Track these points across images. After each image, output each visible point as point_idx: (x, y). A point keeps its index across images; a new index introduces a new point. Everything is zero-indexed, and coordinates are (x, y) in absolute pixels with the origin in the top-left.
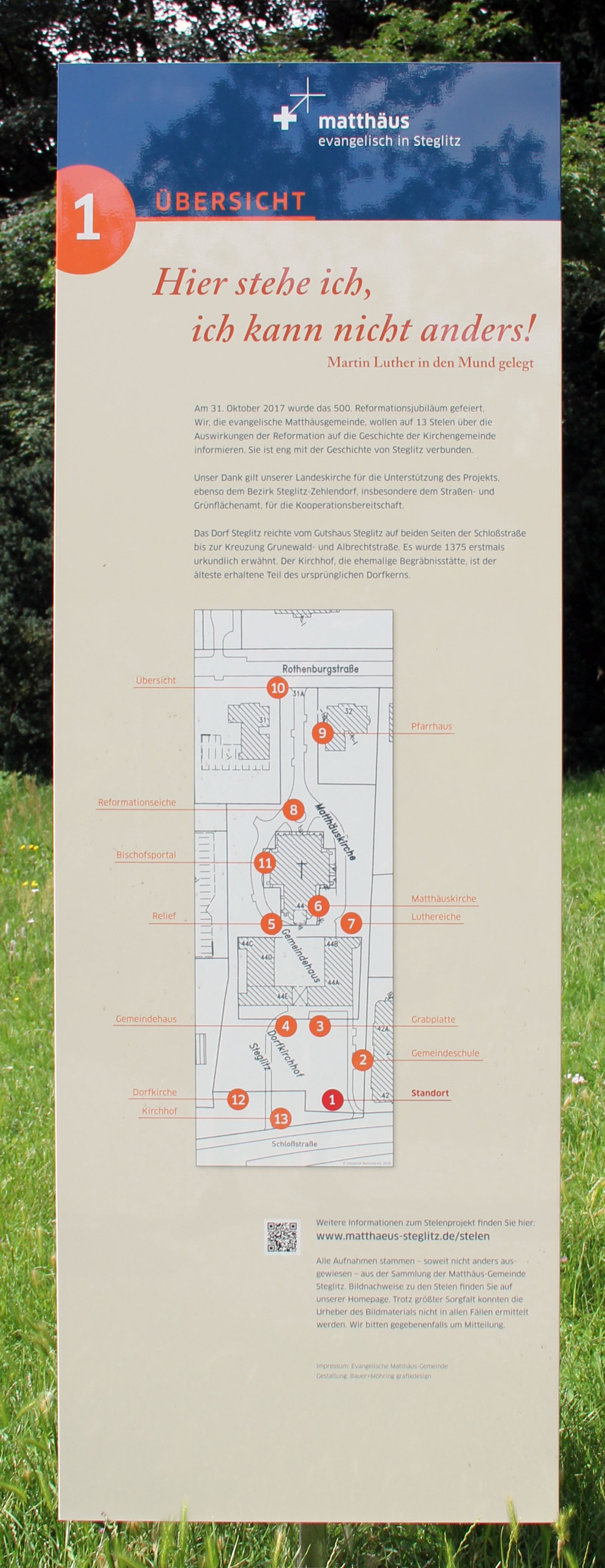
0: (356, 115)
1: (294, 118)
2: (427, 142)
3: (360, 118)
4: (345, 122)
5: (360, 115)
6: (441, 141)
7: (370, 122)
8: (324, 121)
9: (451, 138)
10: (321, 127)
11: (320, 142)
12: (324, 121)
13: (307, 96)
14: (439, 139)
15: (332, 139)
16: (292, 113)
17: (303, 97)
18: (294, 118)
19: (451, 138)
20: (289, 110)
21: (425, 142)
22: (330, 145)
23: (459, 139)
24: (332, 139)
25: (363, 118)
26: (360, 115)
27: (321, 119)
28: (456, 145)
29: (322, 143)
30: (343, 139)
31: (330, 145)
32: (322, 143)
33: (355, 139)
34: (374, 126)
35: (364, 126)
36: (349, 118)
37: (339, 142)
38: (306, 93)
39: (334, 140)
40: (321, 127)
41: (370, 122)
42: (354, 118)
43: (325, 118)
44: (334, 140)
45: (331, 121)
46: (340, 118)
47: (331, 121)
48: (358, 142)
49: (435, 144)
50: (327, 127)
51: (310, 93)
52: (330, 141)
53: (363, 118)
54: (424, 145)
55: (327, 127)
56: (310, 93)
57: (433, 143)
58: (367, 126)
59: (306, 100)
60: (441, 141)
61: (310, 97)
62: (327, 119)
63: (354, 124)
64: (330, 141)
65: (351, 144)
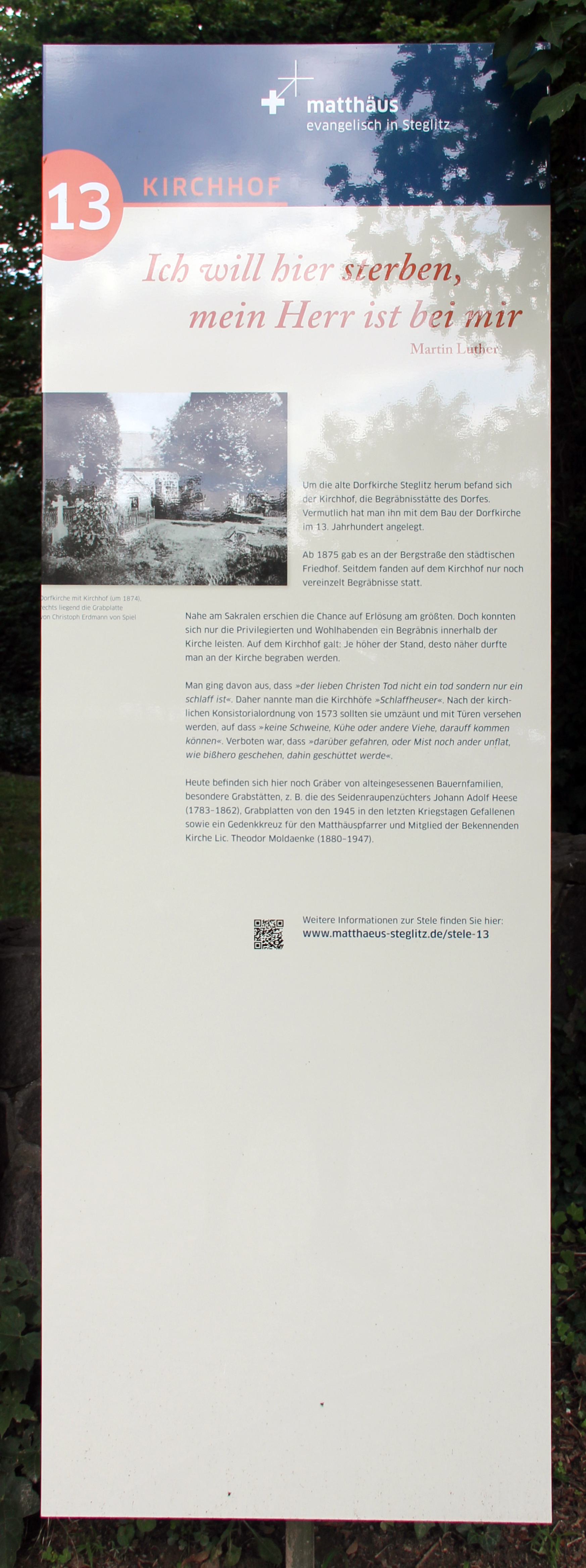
0: (344, 99)
1: (282, 102)
2: (416, 126)
3: (348, 101)
4: (333, 106)
5: (348, 99)
6: (430, 123)
7: (359, 105)
8: (312, 105)
9: (440, 122)
10: (309, 111)
11: (308, 126)
12: (312, 105)
13: (295, 79)
14: (428, 123)
15: (320, 124)
16: (280, 98)
17: (292, 80)
18: (282, 102)
19: (440, 122)
20: (277, 94)
21: (414, 127)
22: (318, 129)
23: (448, 122)
24: (320, 124)
25: (351, 102)
26: (348, 99)
27: (309, 103)
28: (445, 128)
29: (310, 128)
30: (331, 124)
31: (318, 129)
32: (310, 128)
33: (343, 123)
34: (362, 110)
35: (353, 110)
36: (338, 102)
37: (328, 126)
38: (294, 77)
39: (322, 125)
40: (309, 111)
41: (359, 105)
42: (343, 102)
43: (313, 102)
44: (322, 125)
45: (319, 105)
46: (328, 102)
47: (319, 105)
48: (346, 126)
49: (424, 128)
50: (316, 111)
51: (297, 77)
52: (318, 126)
53: (351, 102)
54: (413, 129)
55: (316, 111)
56: (297, 77)
57: (422, 128)
58: (356, 110)
59: (294, 83)
60: (430, 123)
61: (297, 80)
62: (316, 103)
63: (342, 109)
64: (318, 126)
65: (339, 128)
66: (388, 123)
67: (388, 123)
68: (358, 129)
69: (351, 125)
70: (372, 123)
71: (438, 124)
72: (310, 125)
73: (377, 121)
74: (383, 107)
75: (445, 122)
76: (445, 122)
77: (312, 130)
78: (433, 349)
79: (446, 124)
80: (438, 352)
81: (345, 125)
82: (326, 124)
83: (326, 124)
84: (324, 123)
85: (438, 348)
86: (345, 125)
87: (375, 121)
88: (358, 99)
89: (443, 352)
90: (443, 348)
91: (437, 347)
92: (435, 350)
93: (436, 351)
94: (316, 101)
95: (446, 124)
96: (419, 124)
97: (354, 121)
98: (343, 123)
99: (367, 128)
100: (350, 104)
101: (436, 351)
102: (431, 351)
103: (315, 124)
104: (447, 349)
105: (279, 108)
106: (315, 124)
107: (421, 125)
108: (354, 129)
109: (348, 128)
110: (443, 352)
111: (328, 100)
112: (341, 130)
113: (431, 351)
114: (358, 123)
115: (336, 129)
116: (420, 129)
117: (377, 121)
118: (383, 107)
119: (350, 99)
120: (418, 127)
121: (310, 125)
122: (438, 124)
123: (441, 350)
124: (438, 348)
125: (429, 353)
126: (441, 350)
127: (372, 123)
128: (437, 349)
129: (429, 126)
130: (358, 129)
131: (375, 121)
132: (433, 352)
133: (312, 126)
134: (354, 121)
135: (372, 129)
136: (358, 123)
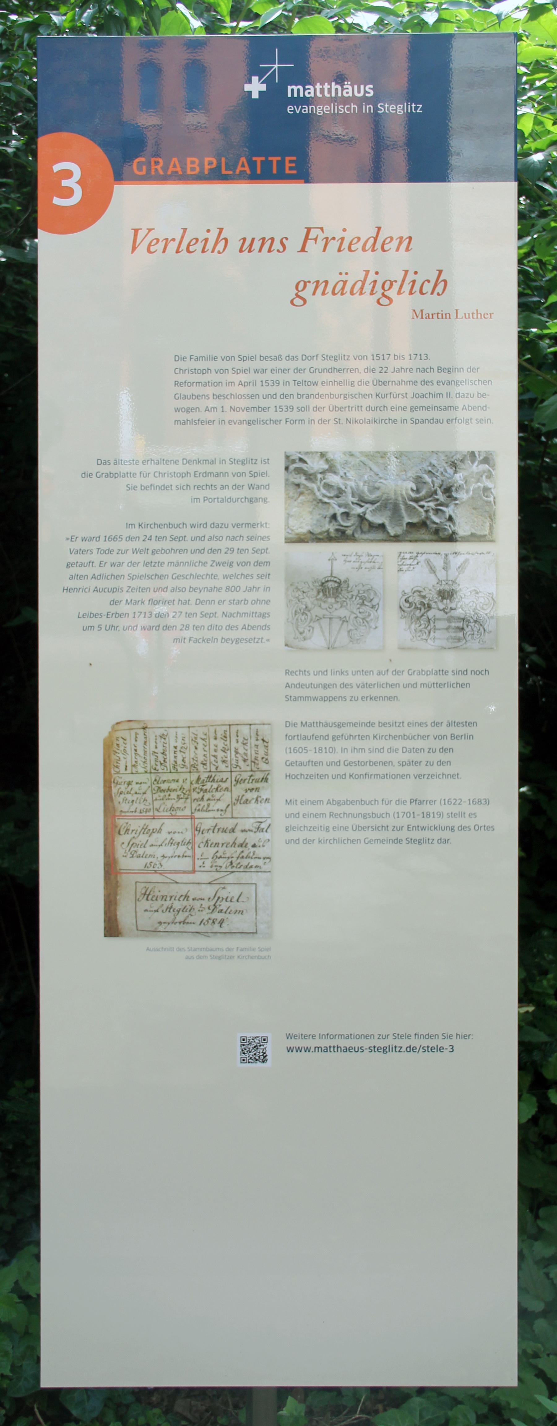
0: (322, 84)
1: (263, 87)
3: (326, 86)
4: (312, 91)
5: (326, 84)
6: (404, 107)
7: (336, 90)
8: (292, 90)
9: (413, 105)
10: (289, 95)
11: (288, 109)
12: (292, 90)
13: (276, 66)
14: (402, 106)
15: (300, 107)
16: (262, 83)
17: (273, 67)
18: (263, 87)
19: (413, 105)
20: (259, 80)
22: (298, 112)
24: (300, 107)
25: (329, 87)
26: (326, 84)
27: (290, 88)
28: (418, 111)
29: (290, 111)
30: (310, 107)
31: (298, 112)
32: (290, 111)
33: (321, 107)
34: (340, 95)
35: (331, 95)
36: (316, 87)
37: (307, 109)
38: (275, 64)
39: (302, 108)
40: (289, 95)
41: (336, 90)
42: (321, 87)
43: (293, 87)
44: (302, 108)
45: (298, 90)
46: (307, 87)
47: (298, 90)
48: (325, 109)
49: (398, 111)
50: (296, 95)
51: (278, 64)
52: (298, 109)
53: (329, 87)
54: (387, 112)
55: (296, 95)
56: (278, 64)
57: (396, 111)
58: (333, 95)
59: (275, 70)
60: (404, 107)
61: (278, 67)
62: (295, 88)
63: (320, 93)
64: (298, 109)
65: (318, 111)
66: (364, 106)
67: (364, 106)
68: (336, 112)
69: (329, 109)
70: (349, 106)
71: (411, 107)
72: (290, 108)
73: (354, 105)
74: (359, 92)
75: (418, 106)
76: (418, 106)
77: (292, 113)
78: (432, 315)
79: (419, 107)
80: (438, 318)
81: (323, 108)
82: (305, 108)
83: (305, 108)
84: (303, 107)
85: (438, 314)
86: (323, 108)
87: (352, 104)
88: (336, 84)
89: (442, 318)
90: (442, 314)
91: (436, 313)
92: (434, 315)
93: (435, 316)
94: (296, 86)
95: (419, 107)
96: (393, 107)
97: (332, 104)
98: (321, 107)
99: (344, 112)
100: (328, 89)
101: (435, 316)
102: (431, 316)
103: (295, 107)
104: (446, 314)
105: (261, 93)
106: (295, 107)
107: (395, 108)
108: (332, 112)
109: (326, 111)
110: (442, 318)
111: (306, 85)
112: (320, 113)
113: (431, 316)
114: (336, 107)
115: (315, 112)
116: (394, 112)
117: (354, 105)
118: (359, 92)
119: (328, 85)
120: (392, 110)
121: (290, 108)
122: (411, 107)
123: (440, 316)
124: (438, 314)
125: (429, 318)
126: (440, 316)
127: (349, 106)
128: (436, 315)
129: (403, 109)
130: (336, 112)
131: (352, 104)
132: (433, 318)
133: (293, 109)
134: (332, 104)
135: (349, 112)
136: (336, 107)
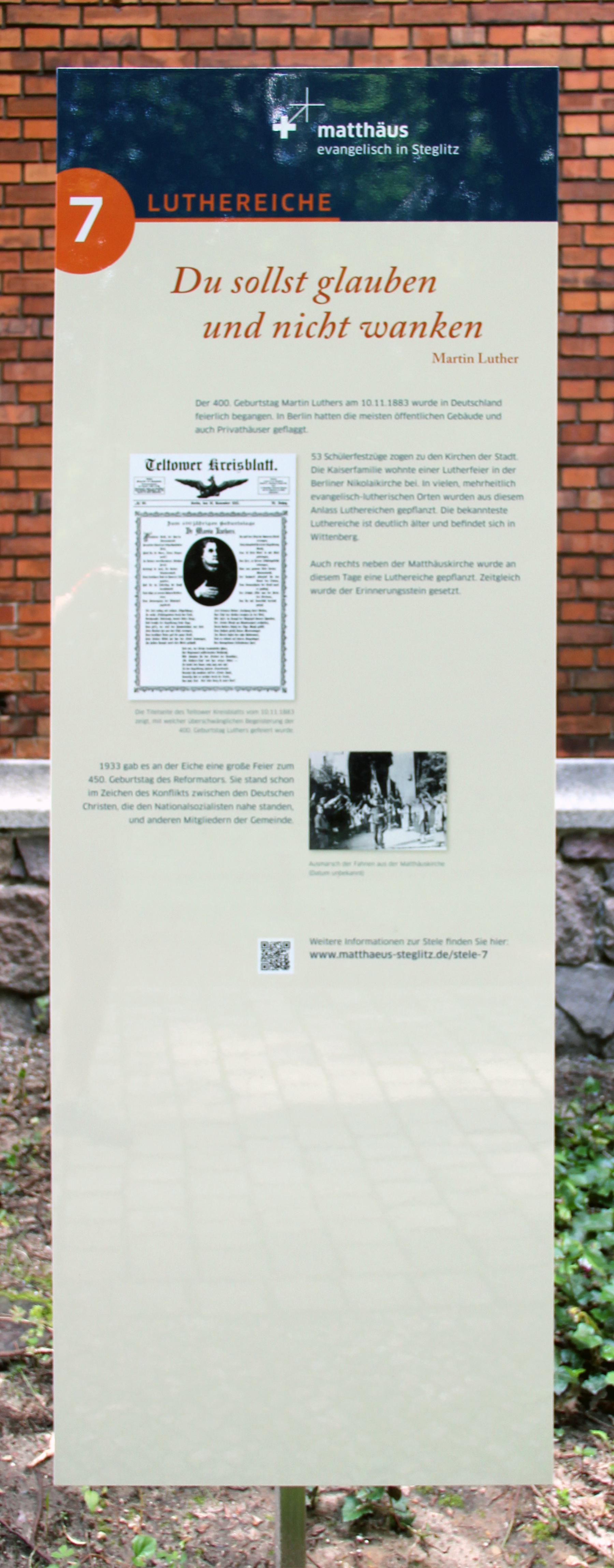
0: (354, 124)
2: (426, 150)
4: (344, 131)
7: (369, 130)
8: (323, 131)
9: (450, 147)
12: (323, 131)
13: (307, 105)
16: (292, 122)
17: (302, 106)
18: (293, 127)
21: (423, 149)
23: (457, 148)
25: (361, 127)
27: (320, 128)
38: (304, 103)
40: (320, 135)
41: (369, 130)
42: (353, 127)
43: (324, 127)
44: (333, 149)
45: (330, 131)
46: (339, 127)
47: (330, 131)
49: (434, 152)
52: (329, 148)
53: (361, 127)
55: (326, 135)
56: (310, 102)
58: (366, 135)
62: (326, 128)
64: (329, 148)
65: (350, 152)
67: (398, 148)
71: (447, 149)
74: (393, 133)
94: (327, 125)
118: (393, 133)
129: (439, 151)
136: (369, 148)
